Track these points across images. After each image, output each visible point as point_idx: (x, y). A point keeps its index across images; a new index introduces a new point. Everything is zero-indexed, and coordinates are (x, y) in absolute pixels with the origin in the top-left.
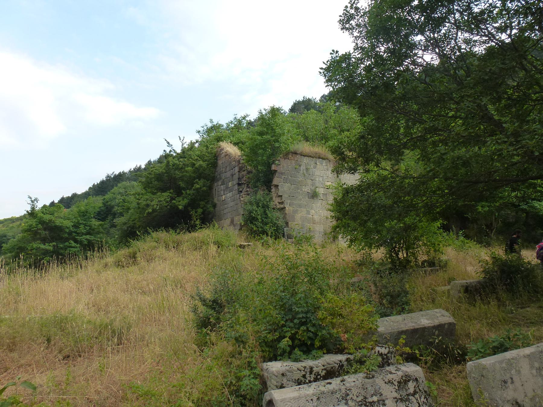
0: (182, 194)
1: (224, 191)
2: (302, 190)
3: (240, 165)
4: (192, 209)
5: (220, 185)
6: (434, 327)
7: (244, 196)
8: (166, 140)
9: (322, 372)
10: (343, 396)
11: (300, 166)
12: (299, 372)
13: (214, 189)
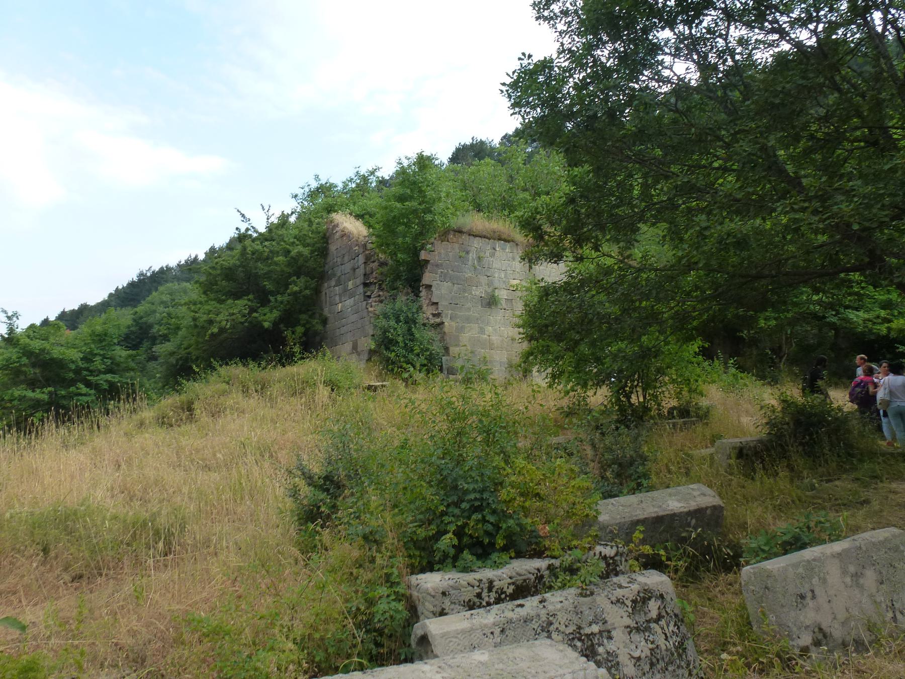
0: (269, 301)
1: (340, 295)
2: (471, 293)
3: (367, 252)
4: (287, 327)
5: (334, 286)
6: (689, 513)
7: (373, 304)
8: (238, 211)
9: (508, 588)
10: (542, 626)
11: (468, 253)
12: (471, 588)
13: (324, 293)
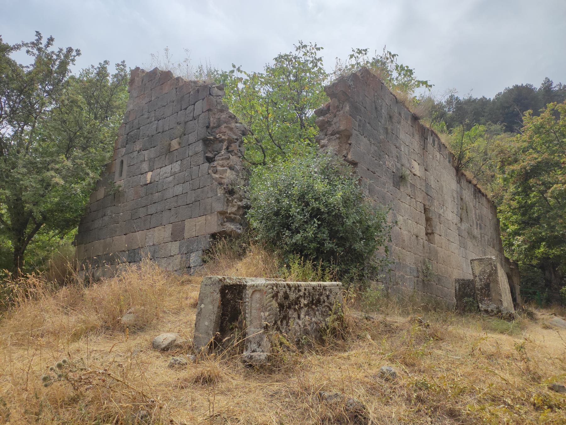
2: (385, 163)
7: (219, 168)
